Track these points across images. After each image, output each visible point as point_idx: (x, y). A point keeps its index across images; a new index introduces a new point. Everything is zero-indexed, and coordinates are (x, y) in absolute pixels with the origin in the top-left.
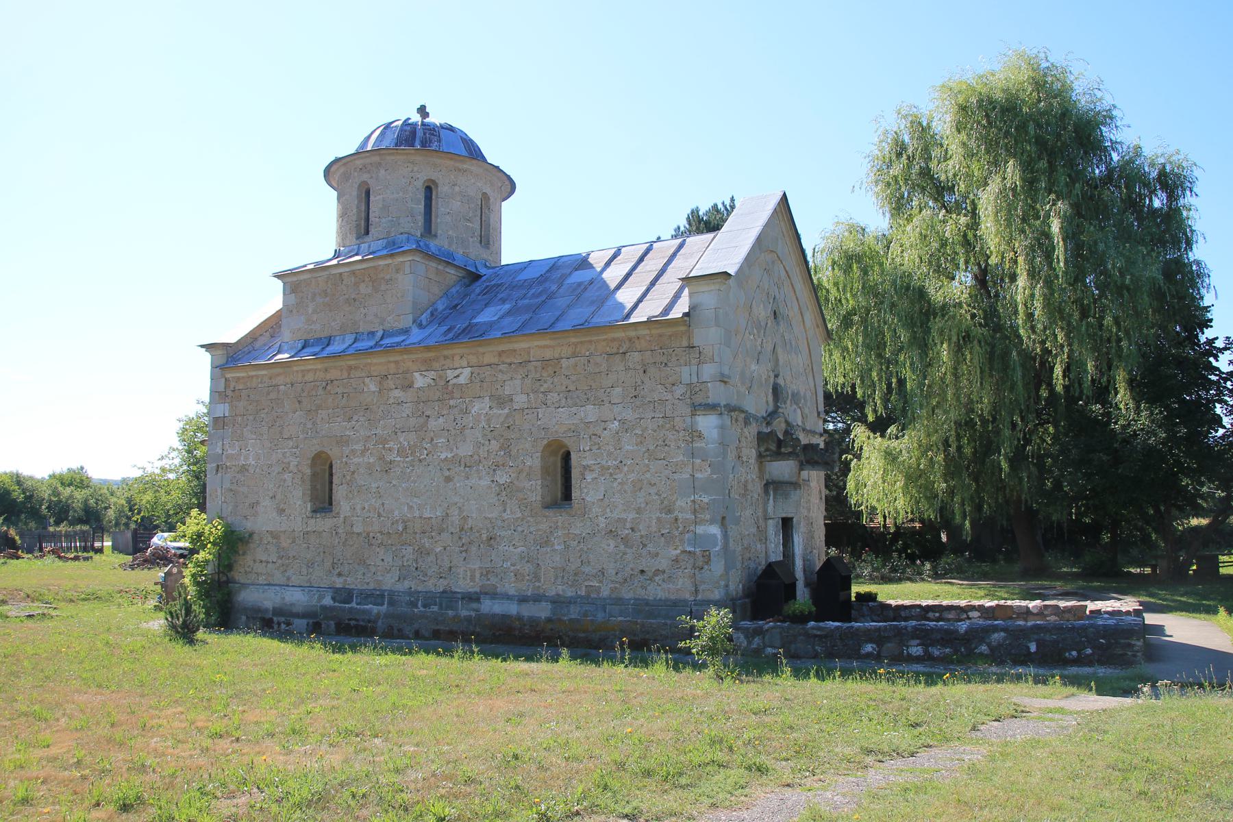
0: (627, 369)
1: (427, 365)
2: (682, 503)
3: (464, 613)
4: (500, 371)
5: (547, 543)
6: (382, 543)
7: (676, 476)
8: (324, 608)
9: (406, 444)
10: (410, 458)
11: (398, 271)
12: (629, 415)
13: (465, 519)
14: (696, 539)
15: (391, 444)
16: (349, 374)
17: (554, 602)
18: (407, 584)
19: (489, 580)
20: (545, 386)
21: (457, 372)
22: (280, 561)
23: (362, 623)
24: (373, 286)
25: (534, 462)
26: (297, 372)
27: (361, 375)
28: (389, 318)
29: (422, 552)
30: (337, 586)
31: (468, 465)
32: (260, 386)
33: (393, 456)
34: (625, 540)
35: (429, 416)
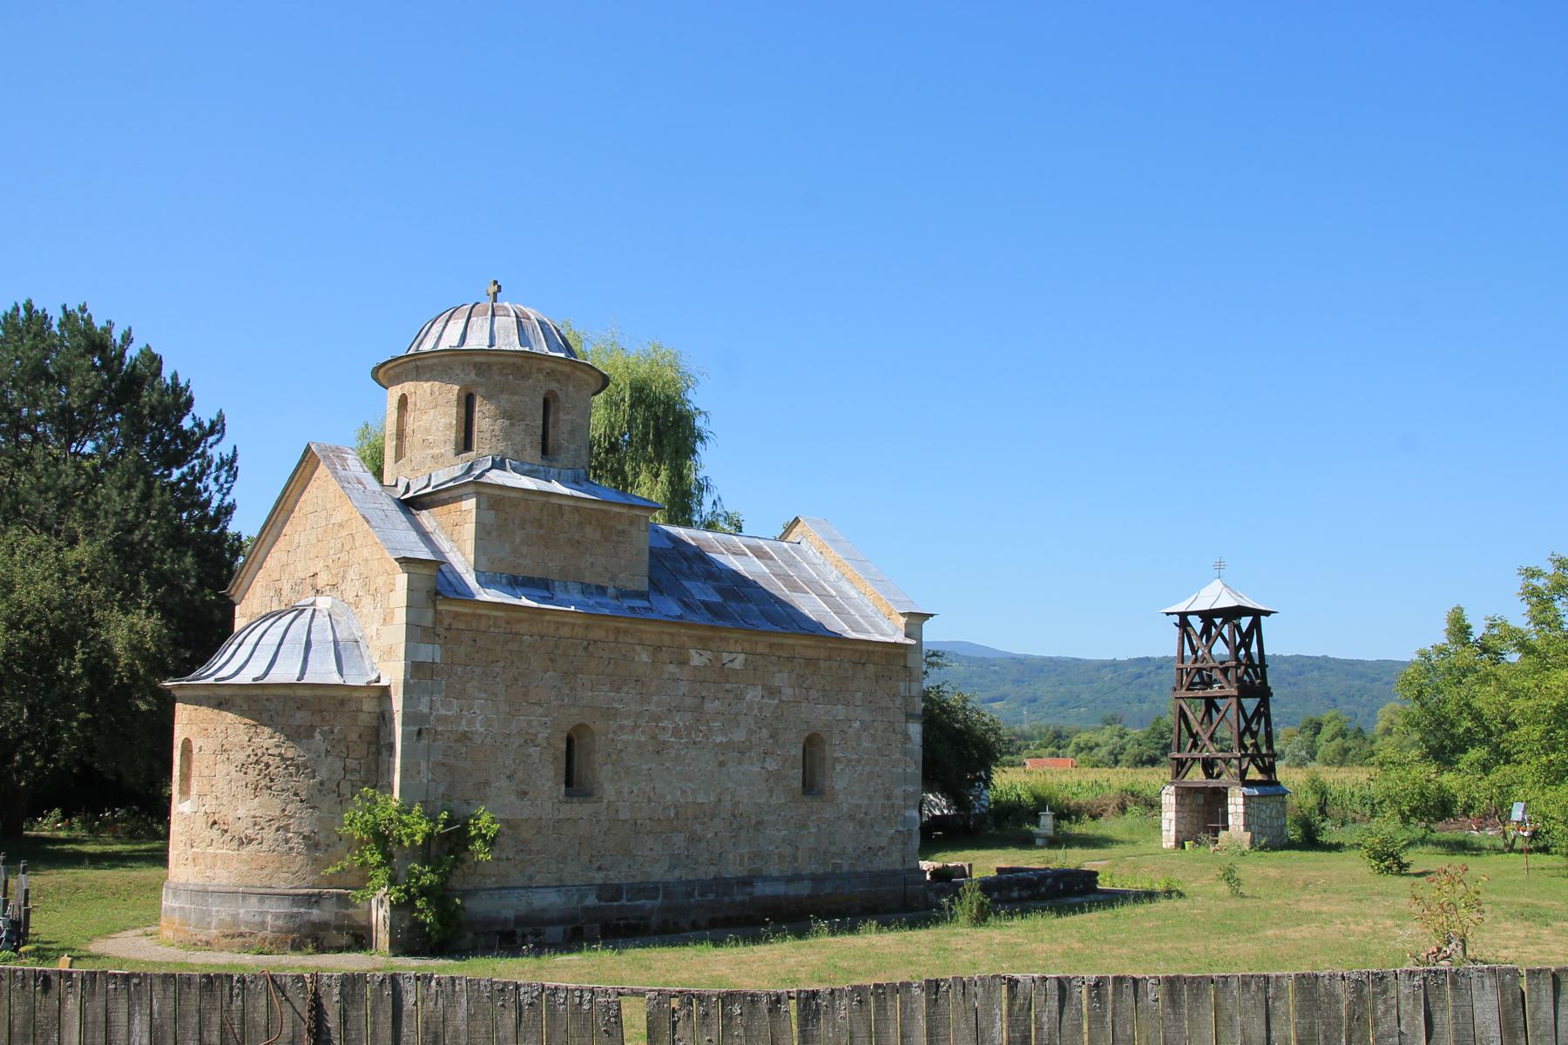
0: (866, 678)
1: (703, 643)
2: (898, 792)
3: (739, 898)
4: (771, 662)
5: (803, 826)
6: (650, 832)
7: (894, 770)
8: (587, 909)
9: (681, 724)
10: (685, 740)
11: (631, 523)
12: (867, 717)
13: (737, 804)
14: (905, 821)
15: (665, 723)
16: (617, 638)
17: (812, 880)
18: (677, 873)
19: (754, 863)
20: (808, 682)
21: (734, 655)
22: (517, 858)
23: (633, 921)
24: (602, 533)
25: (797, 751)
26: (549, 622)
27: (631, 641)
28: (621, 575)
29: (694, 839)
30: (597, 882)
31: (743, 750)
32: (492, 629)
33: (667, 737)
34: (861, 823)
35: (703, 698)
